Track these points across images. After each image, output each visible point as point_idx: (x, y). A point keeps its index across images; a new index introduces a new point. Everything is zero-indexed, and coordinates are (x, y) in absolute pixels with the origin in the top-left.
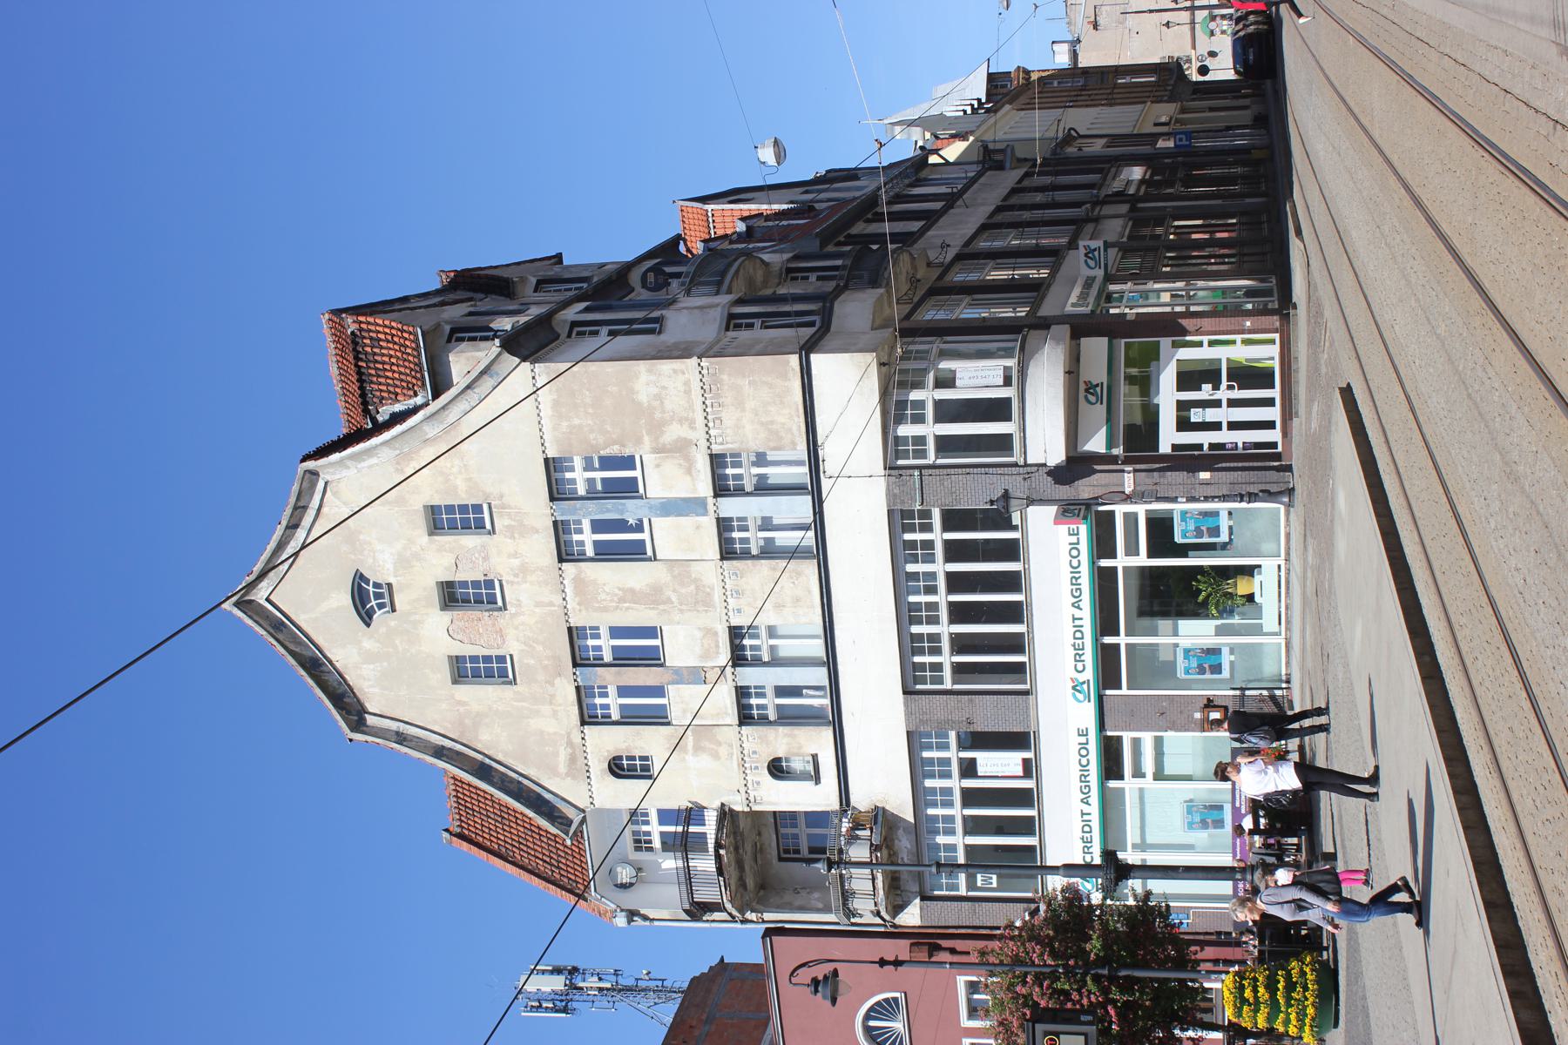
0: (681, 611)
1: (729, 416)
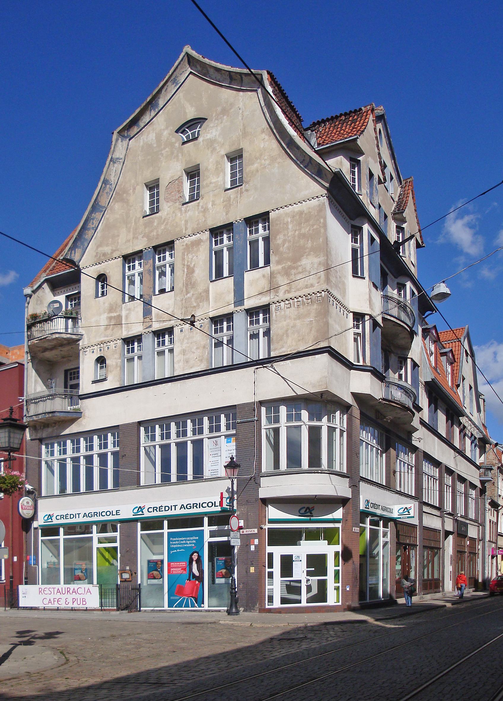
0: (182, 300)
1: (292, 312)
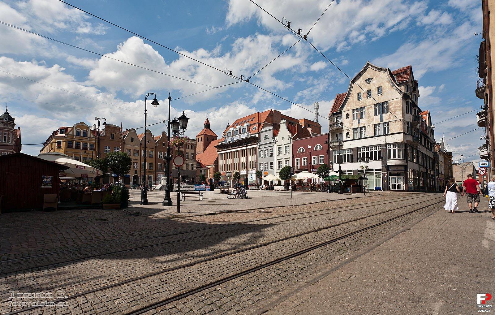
1: (394, 124)
